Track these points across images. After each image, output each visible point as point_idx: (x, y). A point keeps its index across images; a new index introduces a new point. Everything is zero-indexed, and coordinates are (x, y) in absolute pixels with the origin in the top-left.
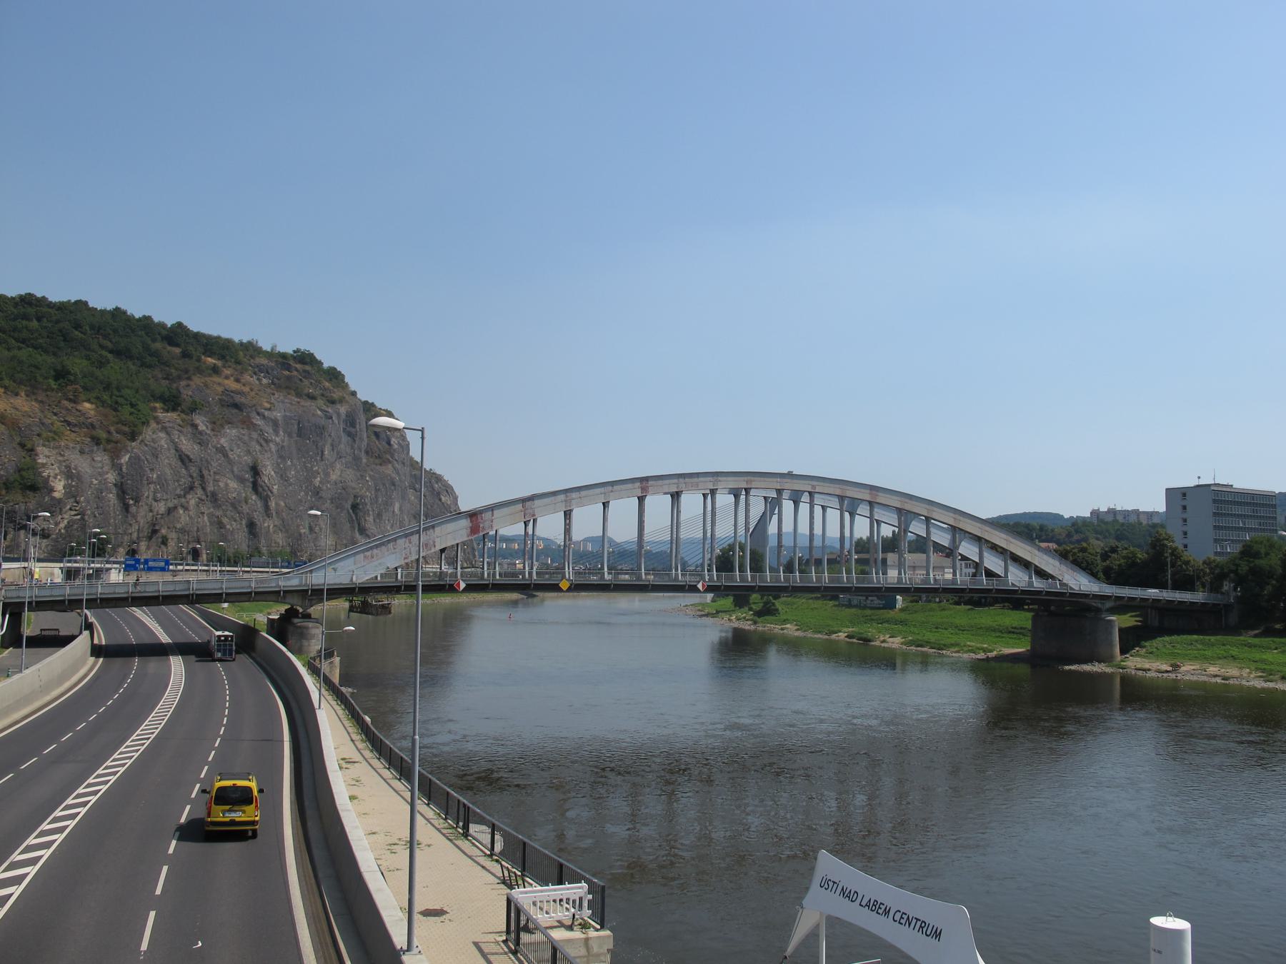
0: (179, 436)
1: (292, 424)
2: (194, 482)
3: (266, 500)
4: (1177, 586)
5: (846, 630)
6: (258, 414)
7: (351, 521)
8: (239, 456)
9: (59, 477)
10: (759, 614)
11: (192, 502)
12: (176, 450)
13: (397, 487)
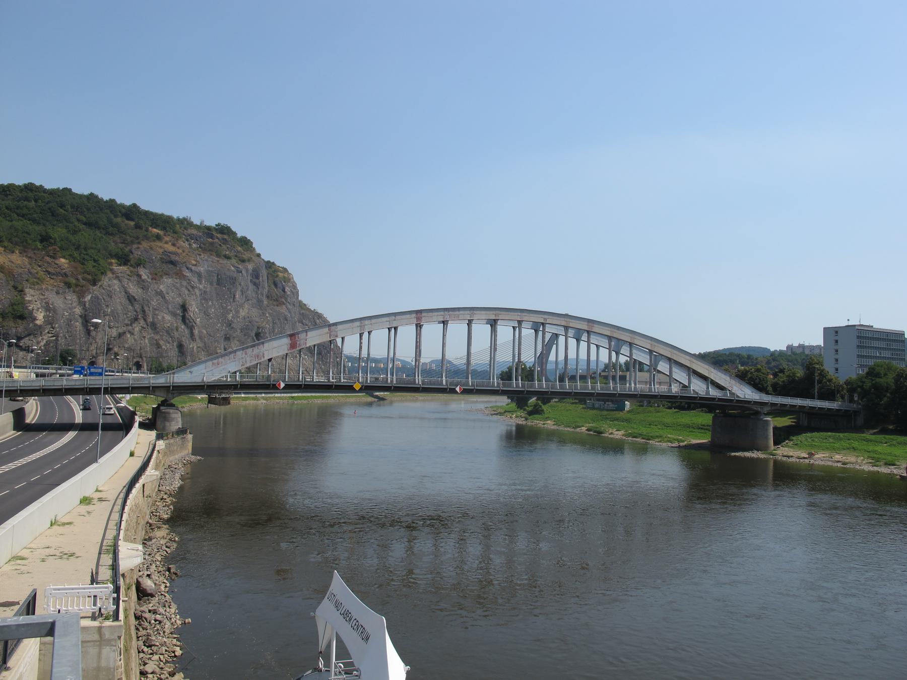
0: (128, 283)
1: (213, 276)
2: (138, 315)
3: (191, 329)
4: (822, 397)
5: (587, 425)
6: (187, 268)
8: (173, 298)
9: (40, 310)
10: (531, 413)
11: (137, 329)
12: (126, 293)
13: (289, 322)
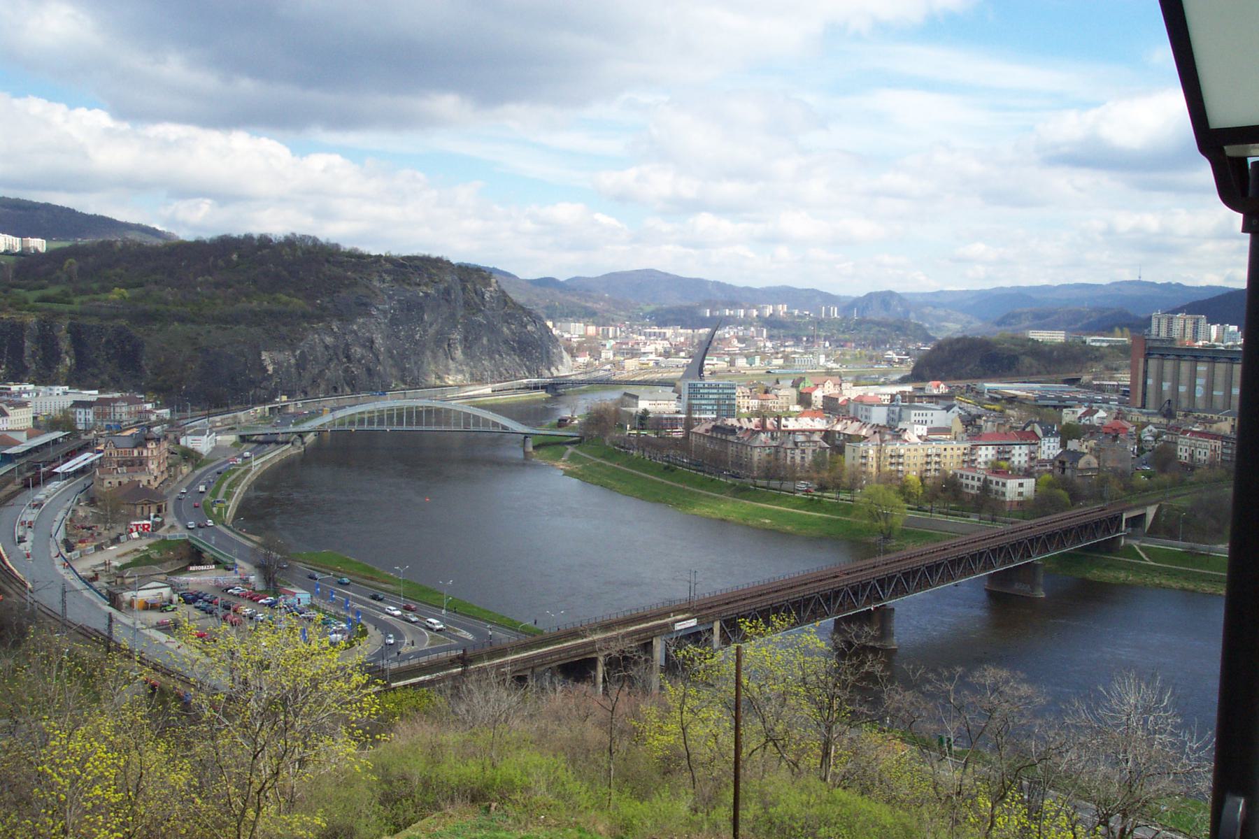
7: (446, 355)
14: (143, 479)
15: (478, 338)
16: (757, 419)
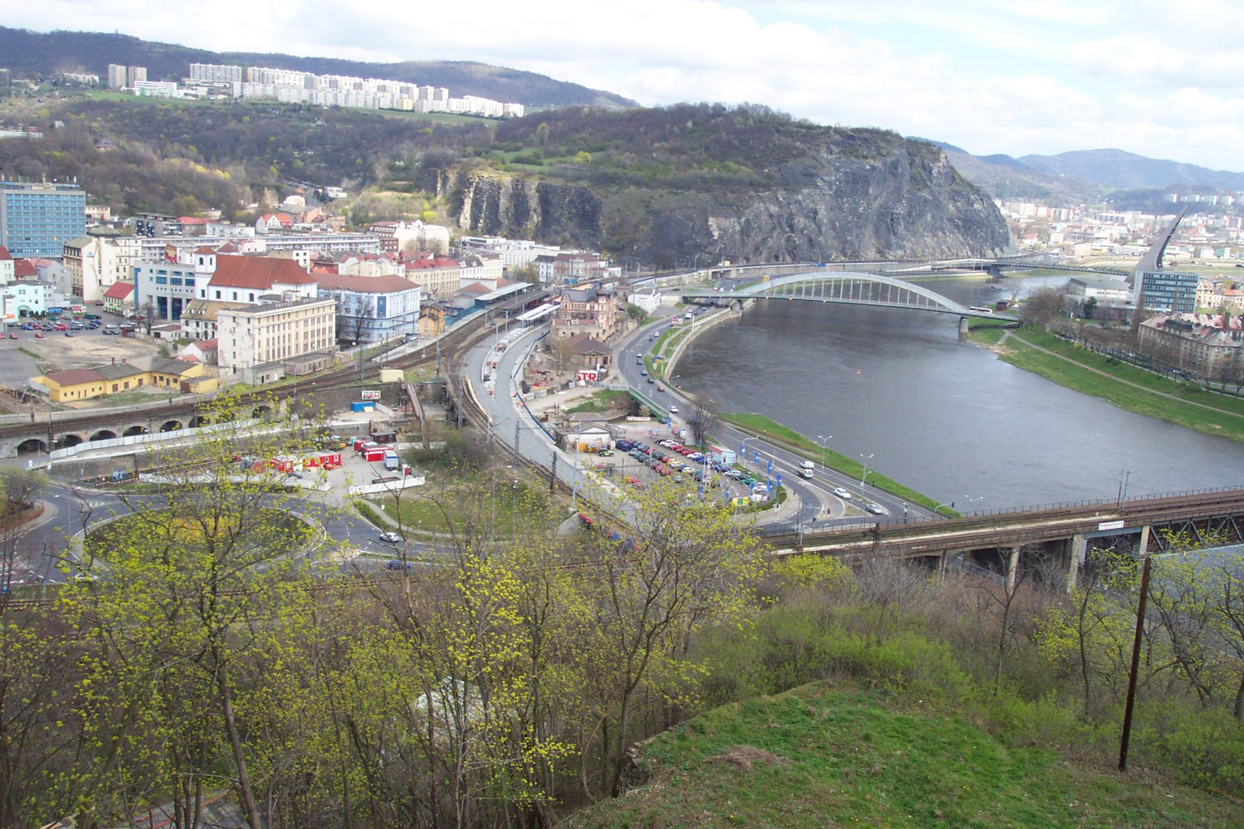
7: (889, 229)
14: (593, 332)
15: (921, 215)
16: (1218, 317)
